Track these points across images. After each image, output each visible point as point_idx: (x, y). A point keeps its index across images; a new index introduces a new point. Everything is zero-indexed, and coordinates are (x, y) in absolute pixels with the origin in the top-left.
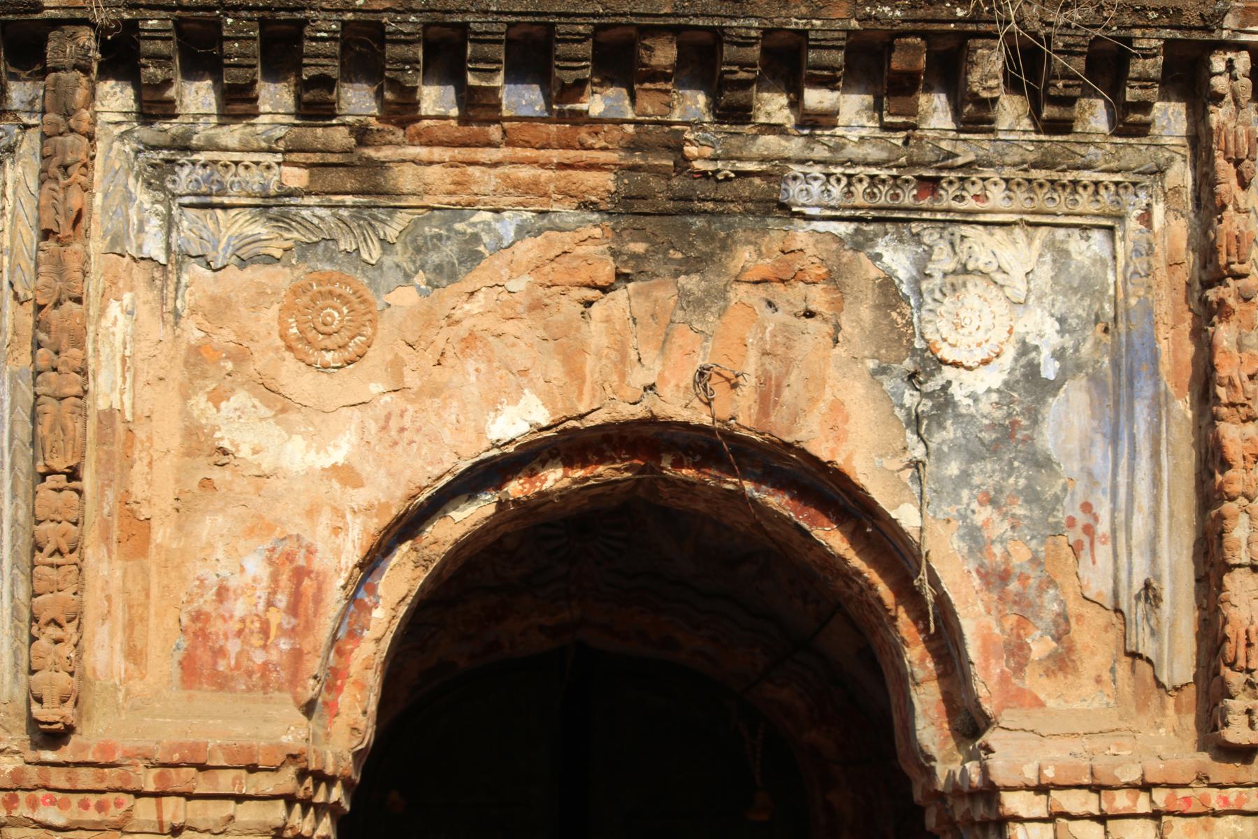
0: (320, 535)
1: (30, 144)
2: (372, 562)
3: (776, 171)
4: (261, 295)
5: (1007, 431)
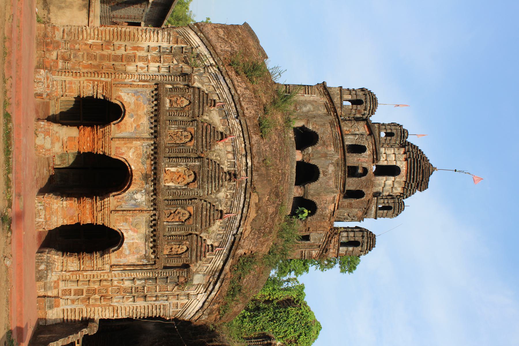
0: (125, 155)
1: (150, 137)
2: (124, 158)
3: (148, 184)
4: (140, 151)
5: (132, 198)
